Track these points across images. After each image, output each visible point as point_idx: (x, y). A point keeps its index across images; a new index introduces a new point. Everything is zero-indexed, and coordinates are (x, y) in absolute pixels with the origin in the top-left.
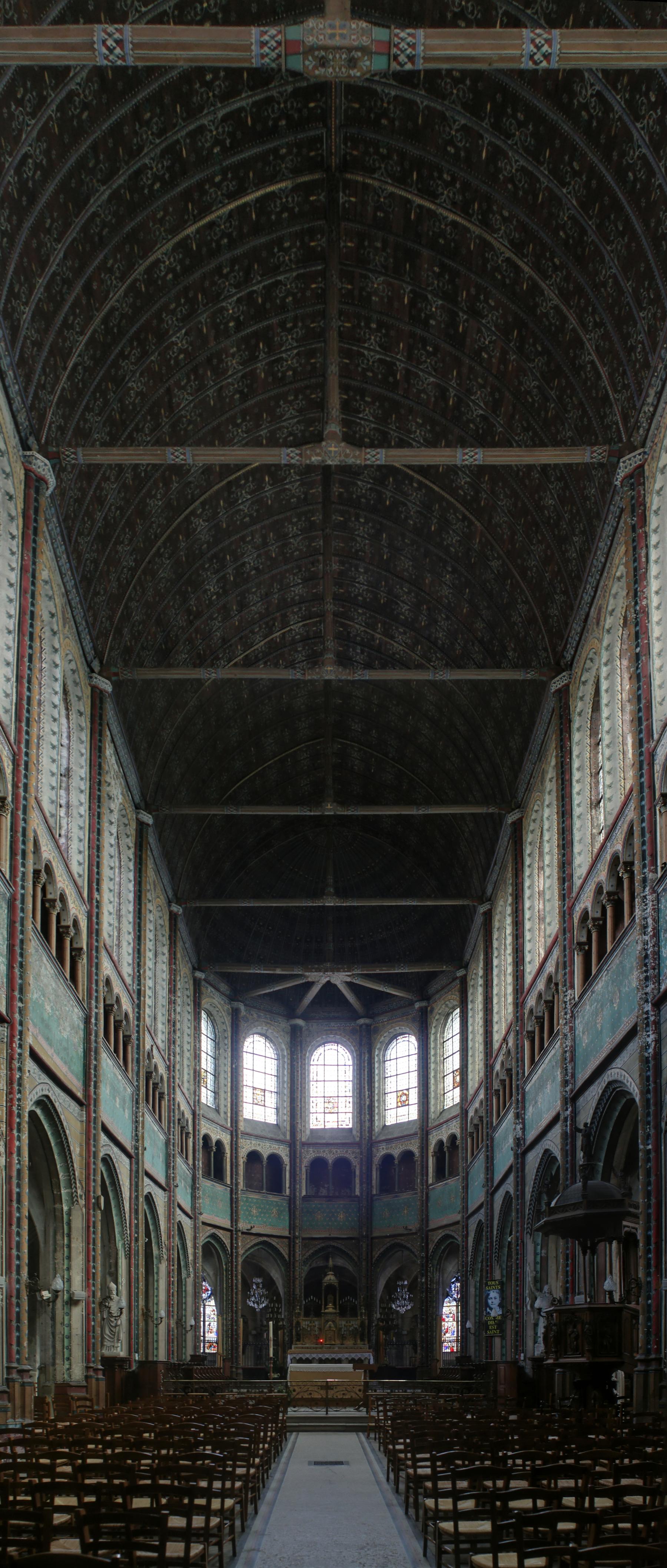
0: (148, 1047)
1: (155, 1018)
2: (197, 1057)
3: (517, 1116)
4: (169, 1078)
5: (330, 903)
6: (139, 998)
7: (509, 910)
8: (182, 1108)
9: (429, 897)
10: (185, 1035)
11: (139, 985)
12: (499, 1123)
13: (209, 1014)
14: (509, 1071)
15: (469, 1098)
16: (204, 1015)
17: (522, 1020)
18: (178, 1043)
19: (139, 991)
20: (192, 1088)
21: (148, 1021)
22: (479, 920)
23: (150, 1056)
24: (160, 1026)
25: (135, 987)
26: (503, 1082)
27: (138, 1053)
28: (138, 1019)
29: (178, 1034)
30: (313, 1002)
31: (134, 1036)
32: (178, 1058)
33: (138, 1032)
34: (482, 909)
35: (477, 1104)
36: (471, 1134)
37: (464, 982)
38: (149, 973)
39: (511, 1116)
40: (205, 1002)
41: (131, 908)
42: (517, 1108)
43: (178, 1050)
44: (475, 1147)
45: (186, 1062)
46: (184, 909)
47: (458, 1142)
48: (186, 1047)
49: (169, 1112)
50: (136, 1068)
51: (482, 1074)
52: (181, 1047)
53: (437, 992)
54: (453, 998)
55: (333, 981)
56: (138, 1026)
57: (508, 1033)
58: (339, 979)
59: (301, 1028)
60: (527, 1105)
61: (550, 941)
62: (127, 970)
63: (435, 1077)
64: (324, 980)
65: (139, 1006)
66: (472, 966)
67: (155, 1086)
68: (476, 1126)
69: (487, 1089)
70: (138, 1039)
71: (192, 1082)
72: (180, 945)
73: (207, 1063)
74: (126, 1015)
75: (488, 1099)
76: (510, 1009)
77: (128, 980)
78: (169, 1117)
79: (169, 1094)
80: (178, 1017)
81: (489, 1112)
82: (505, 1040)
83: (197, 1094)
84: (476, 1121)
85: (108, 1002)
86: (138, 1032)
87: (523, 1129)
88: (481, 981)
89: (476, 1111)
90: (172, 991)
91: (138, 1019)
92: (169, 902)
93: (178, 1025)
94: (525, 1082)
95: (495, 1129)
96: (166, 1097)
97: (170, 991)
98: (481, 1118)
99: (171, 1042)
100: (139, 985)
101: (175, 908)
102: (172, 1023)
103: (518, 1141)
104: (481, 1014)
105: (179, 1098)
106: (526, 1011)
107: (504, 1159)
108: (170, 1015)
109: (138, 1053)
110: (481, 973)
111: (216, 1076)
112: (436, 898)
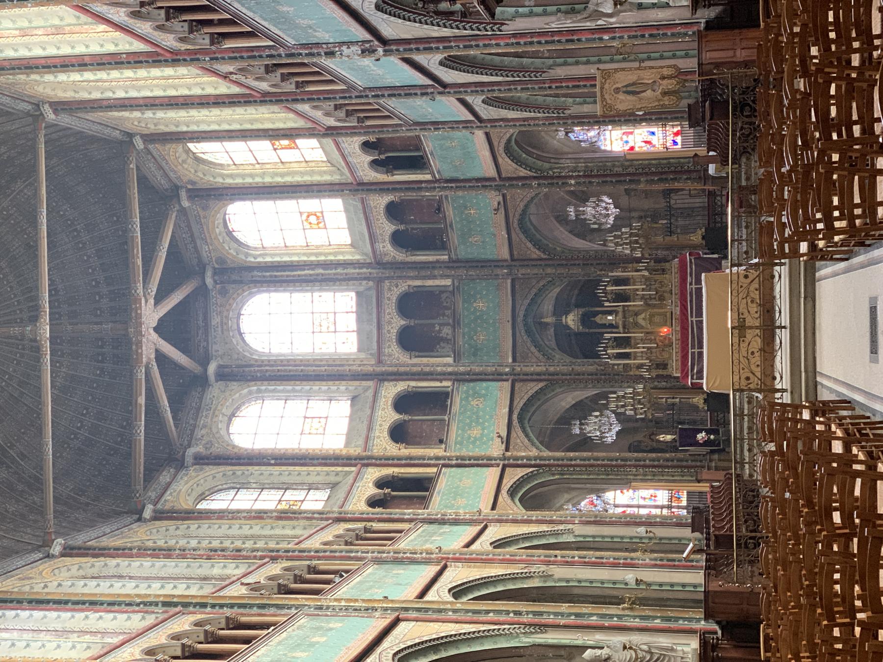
0: (244, 591)
1: (205, 579)
2: (260, 515)
3: (330, 54)
4: (289, 559)
5: (45, 330)
6: (175, 605)
7: (49, 78)
8: (330, 538)
9: (36, 194)
10: (230, 532)
11: (157, 604)
12: (344, 82)
13: (202, 497)
14: (269, 69)
15: (310, 125)
16: (203, 506)
17: (196, 52)
18: (238, 544)
19: (165, 604)
20: (303, 522)
21: (207, 590)
22: (65, 120)
23: (255, 588)
24: (217, 571)
25: (159, 609)
26: (284, 78)
27: (251, 606)
28: (204, 605)
29: (227, 544)
30: (184, 351)
31: (228, 612)
32: (260, 544)
33: (222, 606)
34: (50, 116)
35: (318, 114)
36: (360, 120)
37: (152, 138)
38: (143, 590)
39: (329, 63)
40: (186, 503)
41: (54, 614)
42: (319, 54)
43: (249, 544)
44: (377, 113)
45: (267, 532)
46: (59, 534)
47: (372, 138)
48: (246, 531)
49: (335, 558)
50: (272, 610)
51: (276, 108)
52: (246, 538)
53: (166, 175)
54: (173, 152)
55: (154, 324)
56: (213, 606)
57: (215, 73)
58: (150, 314)
59: (220, 367)
60: (315, 41)
61: (84, 18)
62: (136, 621)
63: (282, 175)
64: (154, 336)
65: (186, 605)
66: (129, 127)
67: (298, 579)
68: (349, 114)
69: (296, 101)
70: (232, 606)
71: (295, 523)
72: (105, 542)
73: (269, 500)
74: (197, 624)
75: (310, 98)
76: (182, 70)
77: (151, 620)
78: (342, 558)
79: (310, 558)
80: (205, 543)
81: (327, 96)
82: (225, 77)
83: (311, 516)
84: (342, 114)
85: (179, 653)
86: (222, 606)
87: (349, 44)
88: (149, 114)
89: (327, 114)
90: (167, 553)
91: (204, 605)
92: (48, 556)
93: (216, 544)
94: (282, 45)
95: (351, 87)
96: (315, 562)
97: (168, 557)
98: (336, 107)
99: (237, 555)
100: (157, 604)
101: (56, 549)
102: (212, 554)
103: (367, 51)
104: (193, 112)
105: (314, 543)
106: (184, 47)
107: (392, 71)
108: (201, 557)
109: (251, 606)
110: (137, 114)
111: (286, 487)
112: (37, 180)
